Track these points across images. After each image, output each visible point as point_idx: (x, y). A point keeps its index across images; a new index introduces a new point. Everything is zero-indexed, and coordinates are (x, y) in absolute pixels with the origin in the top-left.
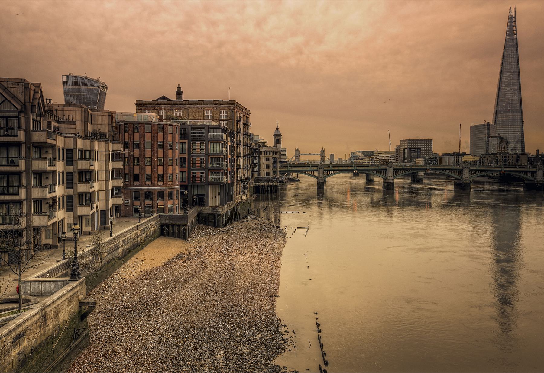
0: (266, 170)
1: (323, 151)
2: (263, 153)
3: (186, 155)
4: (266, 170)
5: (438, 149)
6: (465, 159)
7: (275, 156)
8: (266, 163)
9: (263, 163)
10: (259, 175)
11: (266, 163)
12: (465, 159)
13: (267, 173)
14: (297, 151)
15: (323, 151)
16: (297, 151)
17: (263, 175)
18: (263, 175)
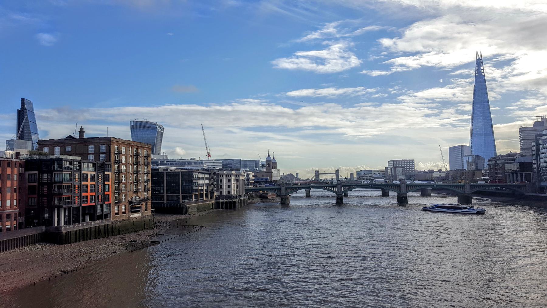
0: (228, 189)
1: (337, 171)
2: (224, 176)
3: (36, 184)
4: (228, 189)
7: (237, 178)
8: (228, 184)
9: (225, 184)
10: (221, 192)
11: (228, 184)
12: (434, 175)
13: (229, 191)
14: (317, 172)
15: (337, 171)
16: (317, 172)
17: (225, 193)
18: (225, 193)
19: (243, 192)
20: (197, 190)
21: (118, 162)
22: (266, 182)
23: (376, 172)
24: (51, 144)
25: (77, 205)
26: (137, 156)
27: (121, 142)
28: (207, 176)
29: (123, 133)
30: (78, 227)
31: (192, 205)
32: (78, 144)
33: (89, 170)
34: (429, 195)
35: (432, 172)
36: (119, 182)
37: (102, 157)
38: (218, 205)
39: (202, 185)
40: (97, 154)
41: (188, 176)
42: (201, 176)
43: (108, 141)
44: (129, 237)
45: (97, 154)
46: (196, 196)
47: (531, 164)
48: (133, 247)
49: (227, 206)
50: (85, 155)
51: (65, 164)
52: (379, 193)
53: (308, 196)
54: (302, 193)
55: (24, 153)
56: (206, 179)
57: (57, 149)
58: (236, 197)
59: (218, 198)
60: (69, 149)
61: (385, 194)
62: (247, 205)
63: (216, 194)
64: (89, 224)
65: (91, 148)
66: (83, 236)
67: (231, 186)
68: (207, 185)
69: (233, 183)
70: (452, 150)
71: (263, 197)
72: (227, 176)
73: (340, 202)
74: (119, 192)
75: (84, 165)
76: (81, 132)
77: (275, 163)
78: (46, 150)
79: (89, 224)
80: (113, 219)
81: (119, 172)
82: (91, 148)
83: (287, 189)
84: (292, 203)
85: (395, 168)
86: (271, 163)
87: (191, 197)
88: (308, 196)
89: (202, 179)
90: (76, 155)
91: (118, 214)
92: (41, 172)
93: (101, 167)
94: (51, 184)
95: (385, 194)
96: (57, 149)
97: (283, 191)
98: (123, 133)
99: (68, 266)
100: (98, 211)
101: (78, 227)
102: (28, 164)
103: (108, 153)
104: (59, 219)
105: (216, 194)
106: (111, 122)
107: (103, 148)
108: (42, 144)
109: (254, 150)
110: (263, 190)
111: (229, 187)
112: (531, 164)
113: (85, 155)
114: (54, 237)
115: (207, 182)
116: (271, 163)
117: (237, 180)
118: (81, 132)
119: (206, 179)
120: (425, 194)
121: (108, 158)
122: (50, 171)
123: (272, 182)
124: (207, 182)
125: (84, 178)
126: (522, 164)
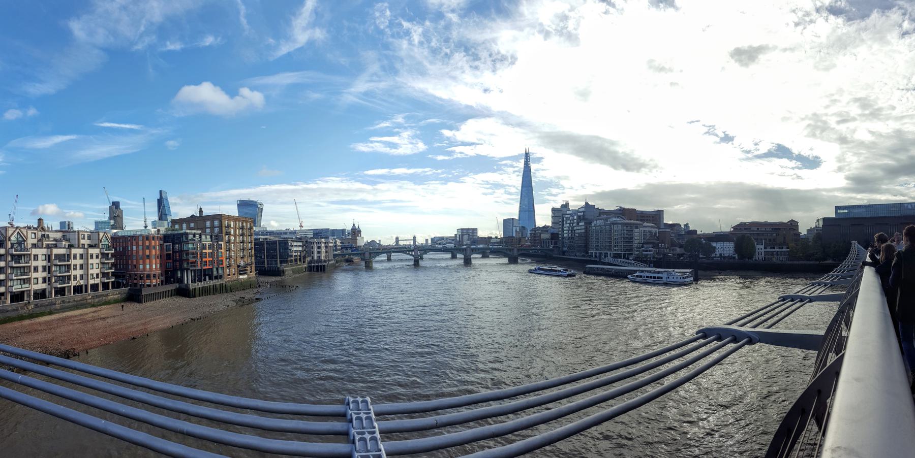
5: (481, 234)
6: (492, 241)
9: (315, 250)
12: (492, 241)
17: (316, 258)
18: (316, 258)
19: (331, 257)
20: (292, 256)
21: (228, 234)
22: (352, 247)
23: (447, 238)
24: (180, 221)
25: (199, 268)
26: (242, 228)
27: (230, 218)
28: (300, 244)
29: (233, 211)
30: (200, 285)
31: (288, 269)
32: (199, 220)
33: (207, 241)
34: (488, 257)
35: (491, 238)
36: (229, 250)
37: (216, 230)
38: (310, 269)
39: (296, 251)
40: (212, 227)
41: (284, 244)
42: (295, 244)
43: (220, 217)
44: (239, 295)
45: (212, 227)
46: (291, 261)
47: (558, 234)
48: (242, 302)
49: (318, 269)
50: (203, 229)
51: (190, 237)
52: (449, 256)
53: (389, 260)
54: (384, 257)
55: (163, 230)
56: (300, 246)
57: (184, 226)
58: (325, 261)
59: (309, 263)
60: (192, 225)
61: (454, 257)
62: (335, 268)
63: (308, 259)
64: (209, 283)
65: (208, 224)
66: (205, 292)
67: (321, 252)
68: (300, 251)
69: (323, 249)
70: (506, 222)
71: (349, 261)
72: (318, 243)
73: (416, 264)
74: (230, 258)
75: (204, 237)
76: (201, 211)
77: (360, 232)
78: (177, 227)
79: (209, 283)
80: (226, 279)
81: (229, 241)
82: (208, 224)
83: (370, 254)
84: (375, 265)
85: (463, 235)
86: (356, 232)
87: (287, 262)
88: (389, 260)
89: (296, 246)
90: (198, 229)
91: (230, 276)
92: (174, 243)
93: (216, 238)
94: (181, 252)
95: (454, 257)
96: (184, 226)
97: (367, 256)
98: (233, 211)
99: (196, 316)
100: (215, 273)
101: (200, 285)
102: (166, 238)
103: (220, 226)
104: (188, 278)
105: (308, 259)
106: (223, 202)
107: (216, 223)
108: (174, 222)
109: (341, 221)
110: (349, 255)
111: (319, 252)
112: (558, 234)
113: (203, 229)
114: (184, 292)
115: (300, 249)
116: (356, 232)
117: (326, 247)
118: (201, 211)
119: (300, 246)
120: (485, 256)
121: (221, 231)
122: (180, 243)
123: (357, 248)
124: (300, 249)
125: (203, 247)
126: (552, 234)
